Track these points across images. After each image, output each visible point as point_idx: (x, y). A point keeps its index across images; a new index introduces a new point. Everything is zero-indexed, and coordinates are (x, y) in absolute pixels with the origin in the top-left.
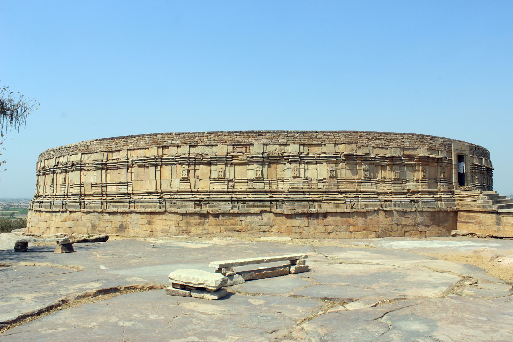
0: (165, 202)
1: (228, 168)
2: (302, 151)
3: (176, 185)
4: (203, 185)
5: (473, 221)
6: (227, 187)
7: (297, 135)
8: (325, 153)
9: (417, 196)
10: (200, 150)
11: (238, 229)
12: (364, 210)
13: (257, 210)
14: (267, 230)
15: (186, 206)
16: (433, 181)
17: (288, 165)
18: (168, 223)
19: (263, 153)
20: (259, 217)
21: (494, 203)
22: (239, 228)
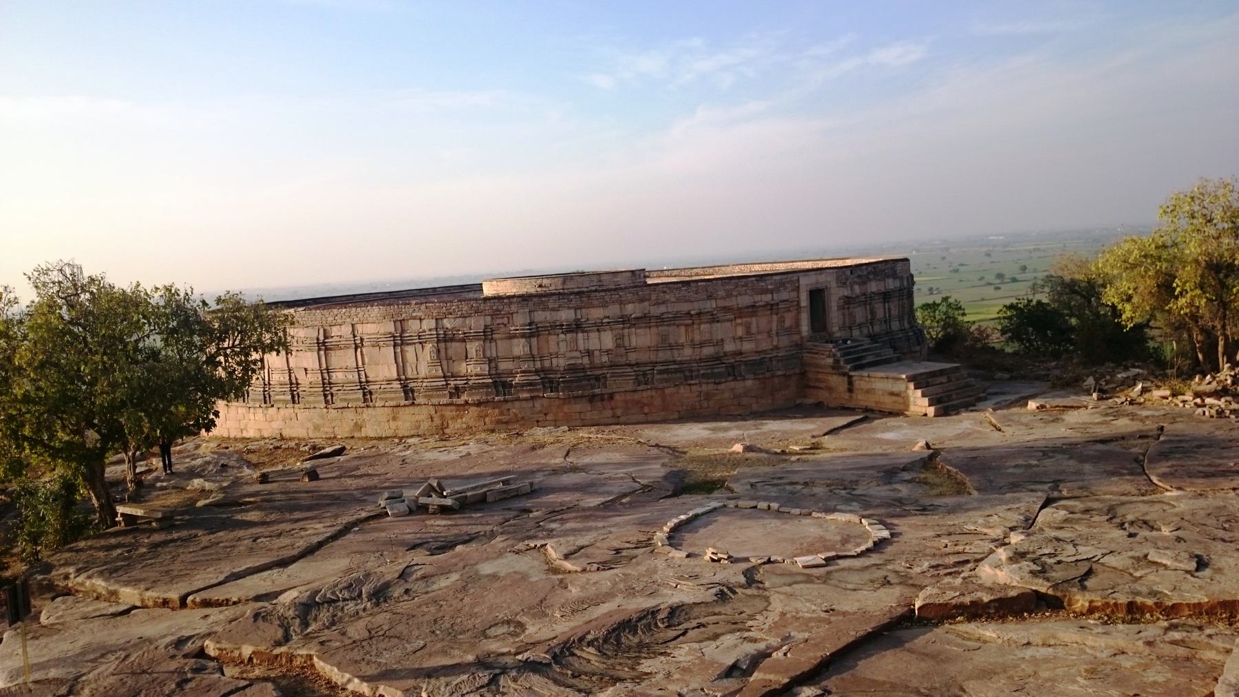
1: (488, 344)
3: (424, 370)
12: (661, 386)
15: (438, 396)
16: (765, 336)
17: (562, 336)
18: (418, 418)
19: (530, 324)
20: (530, 404)
21: (847, 362)
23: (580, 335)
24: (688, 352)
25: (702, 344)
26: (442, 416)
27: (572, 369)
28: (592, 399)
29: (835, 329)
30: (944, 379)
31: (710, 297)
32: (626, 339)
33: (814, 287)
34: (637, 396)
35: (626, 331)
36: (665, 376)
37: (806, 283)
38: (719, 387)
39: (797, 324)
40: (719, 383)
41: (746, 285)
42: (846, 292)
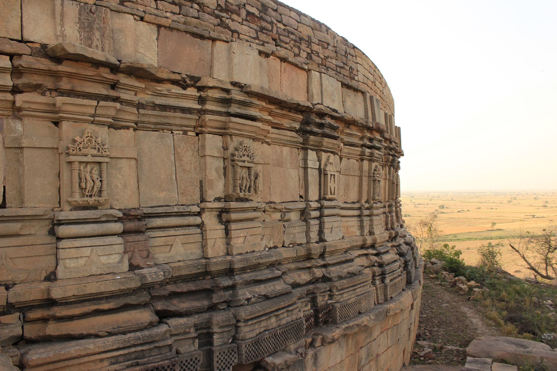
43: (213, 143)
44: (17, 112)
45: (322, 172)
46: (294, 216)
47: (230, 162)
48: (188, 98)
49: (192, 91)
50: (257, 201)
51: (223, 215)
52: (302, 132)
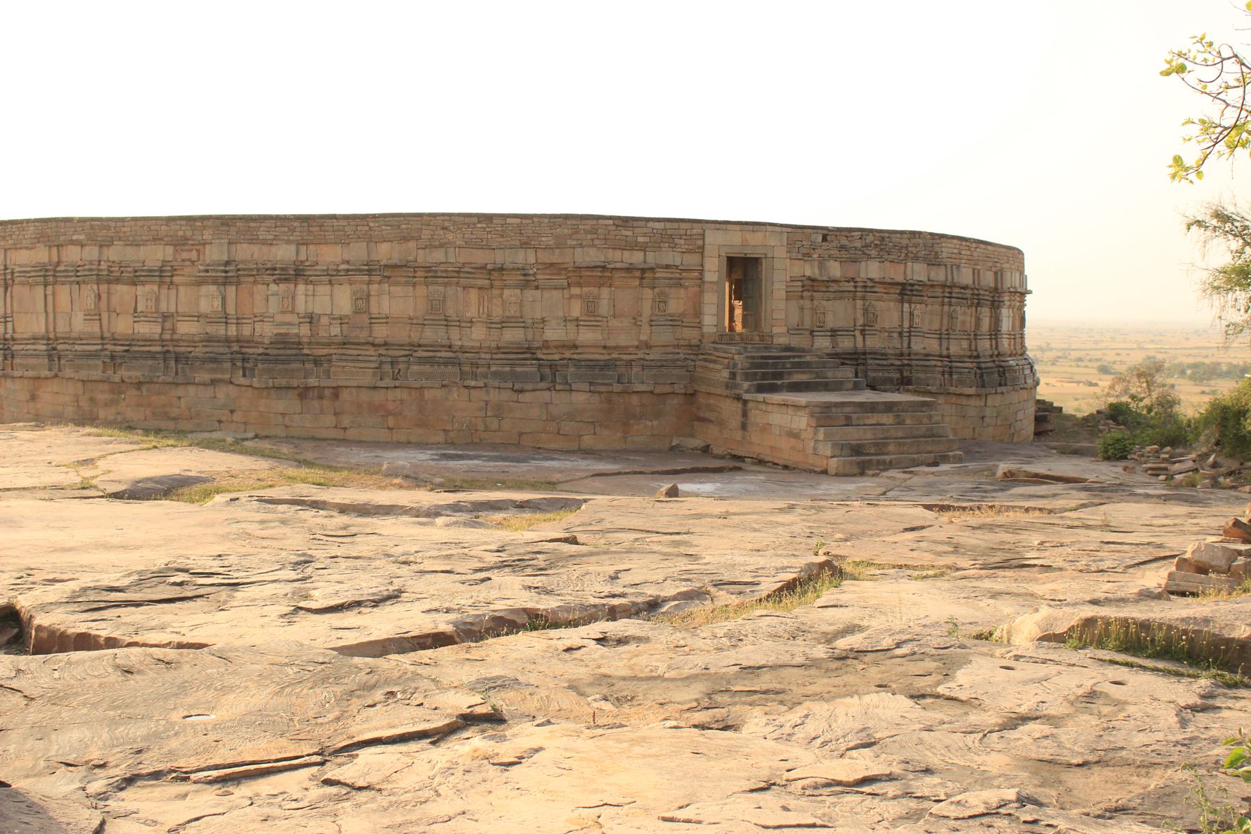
0: (59, 359)
1: (164, 291)
2: (303, 257)
3: (80, 325)
4: (123, 326)
5: (712, 416)
6: (159, 331)
7: (296, 224)
8: (348, 262)
9: (568, 355)
10: (114, 253)
11: (173, 415)
13: (206, 377)
14: (224, 419)
17: (273, 287)
19: (227, 263)
20: (210, 391)
21: (747, 377)
22: (175, 412)
23: (301, 288)
24: (478, 335)
25: (504, 324)
26: (92, 400)
27: (282, 341)
28: (304, 393)
29: (776, 330)
30: (887, 419)
31: (525, 245)
32: (373, 300)
33: (737, 252)
34: (378, 397)
35: (374, 288)
36: (427, 368)
37: (735, 243)
38: (522, 397)
39: (698, 313)
40: (521, 391)
41: (594, 231)
42: (809, 270)
43: (859, 303)
44: (802, 297)
45: (911, 314)
46: (895, 335)
47: (866, 311)
48: (850, 286)
49: (852, 284)
50: (877, 327)
51: (863, 332)
52: (900, 294)
